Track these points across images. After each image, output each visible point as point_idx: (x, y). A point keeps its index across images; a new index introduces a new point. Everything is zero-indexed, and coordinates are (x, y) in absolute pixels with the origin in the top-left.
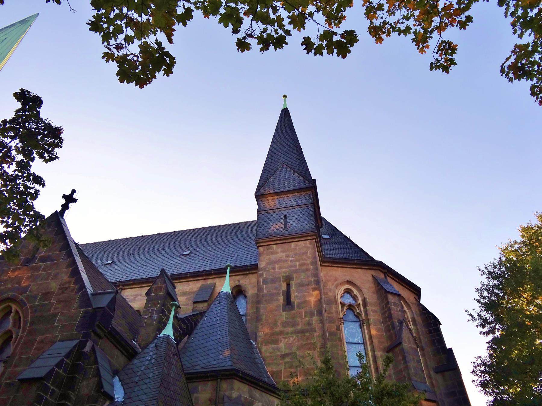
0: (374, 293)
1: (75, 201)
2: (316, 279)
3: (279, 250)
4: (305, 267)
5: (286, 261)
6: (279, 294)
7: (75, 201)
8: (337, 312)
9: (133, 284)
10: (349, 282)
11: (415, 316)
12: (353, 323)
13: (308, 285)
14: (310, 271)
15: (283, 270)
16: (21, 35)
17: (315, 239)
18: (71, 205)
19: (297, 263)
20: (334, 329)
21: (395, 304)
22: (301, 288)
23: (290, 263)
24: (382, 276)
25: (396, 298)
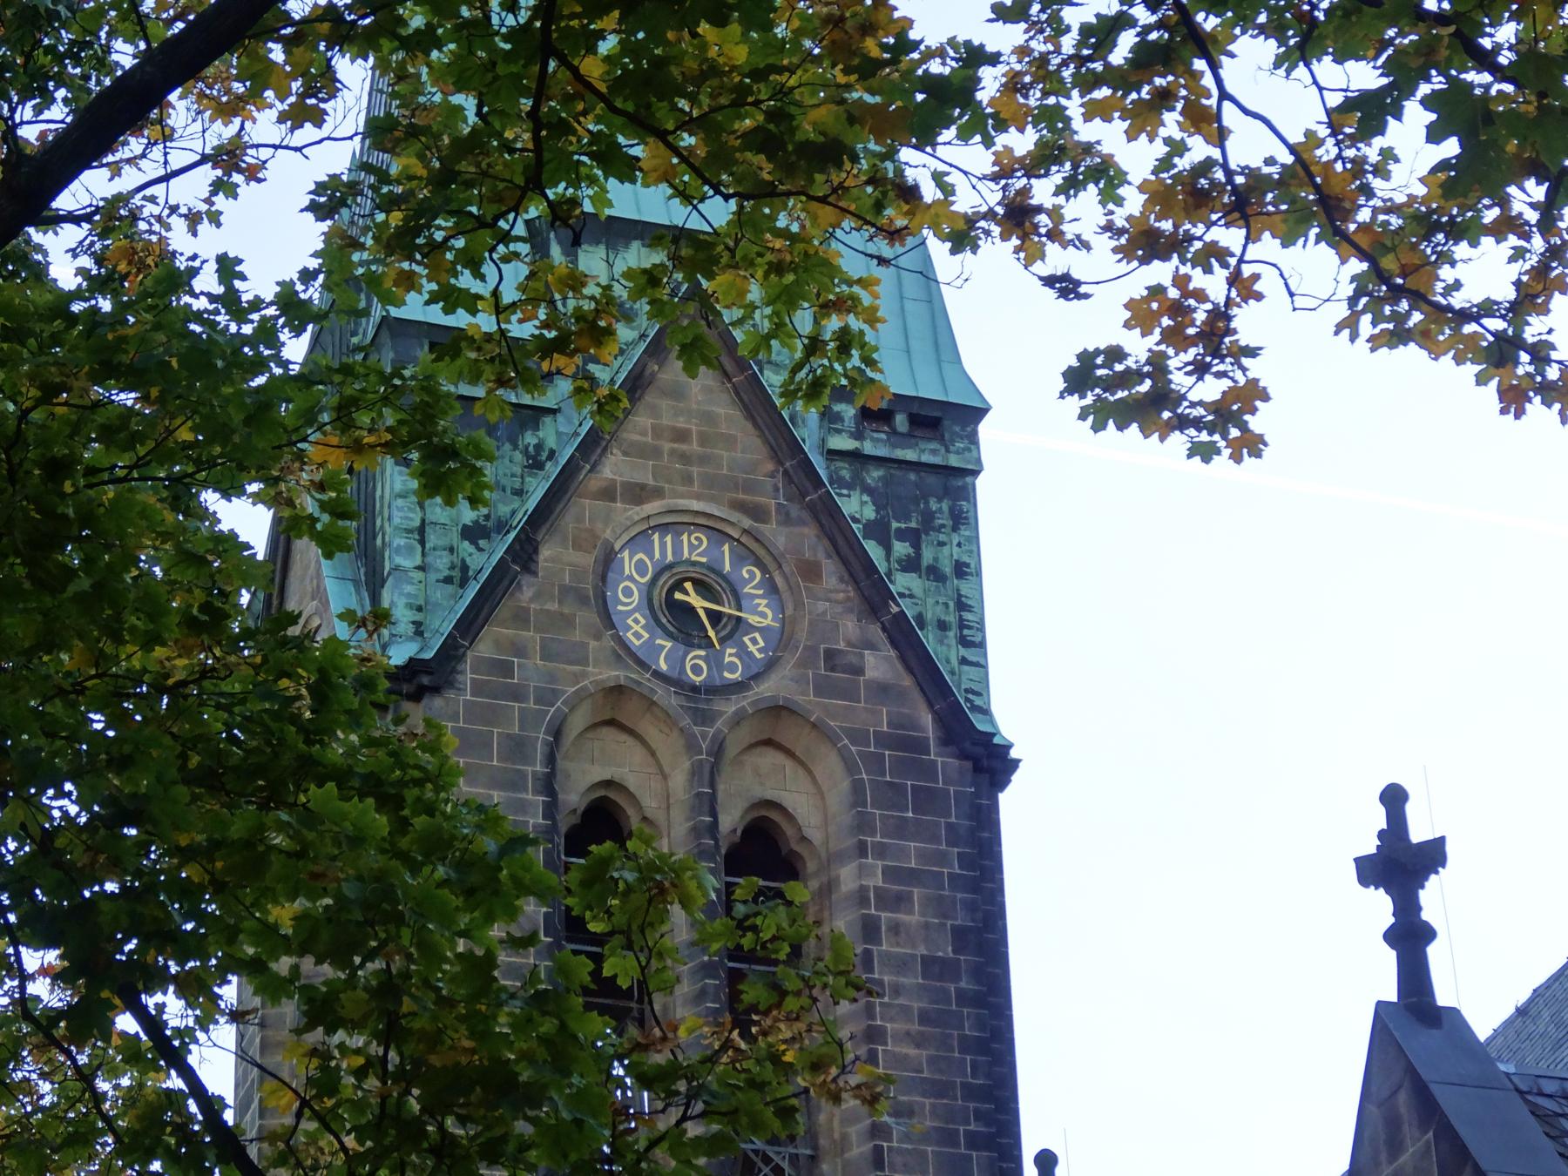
1: (1432, 856)
7: (1432, 856)
18: (1433, 899)
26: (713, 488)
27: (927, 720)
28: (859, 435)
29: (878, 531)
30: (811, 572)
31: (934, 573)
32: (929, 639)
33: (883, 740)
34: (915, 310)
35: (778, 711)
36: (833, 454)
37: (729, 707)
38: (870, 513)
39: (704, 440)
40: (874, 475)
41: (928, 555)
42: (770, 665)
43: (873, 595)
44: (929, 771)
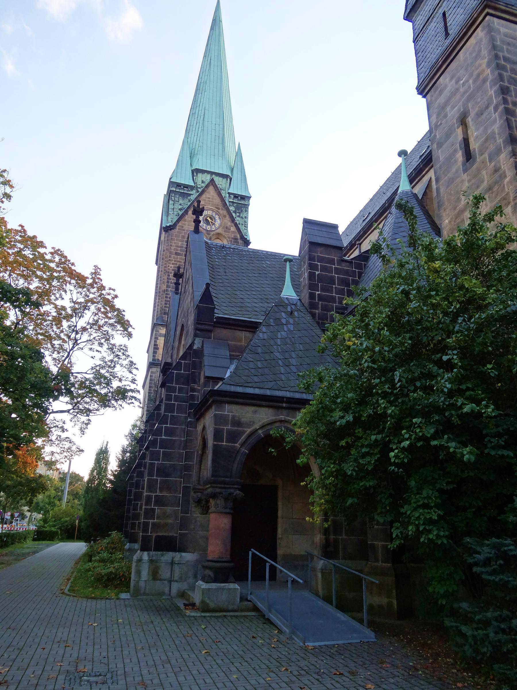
2: (498, 85)
3: (448, 80)
4: (481, 77)
5: (457, 90)
6: (456, 151)
9: (365, 233)
13: (487, 107)
15: (456, 108)
16: (219, 41)
19: (471, 81)
23: (462, 90)
26: (212, 205)
27: (239, 236)
28: (233, 199)
29: (235, 212)
30: (225, 216)
31: (242, 218)
32: (240, 226)
33: (232, 238)
34: (243, 184)
35: (219, 234)
36: (230, 202)
37: (212, 233)
38: (234, 209)
39: (212, 199)
40: (235, 205)
41: (241, 215)
42: (219, 228)
43: (233, 220)
44: (238, 242)
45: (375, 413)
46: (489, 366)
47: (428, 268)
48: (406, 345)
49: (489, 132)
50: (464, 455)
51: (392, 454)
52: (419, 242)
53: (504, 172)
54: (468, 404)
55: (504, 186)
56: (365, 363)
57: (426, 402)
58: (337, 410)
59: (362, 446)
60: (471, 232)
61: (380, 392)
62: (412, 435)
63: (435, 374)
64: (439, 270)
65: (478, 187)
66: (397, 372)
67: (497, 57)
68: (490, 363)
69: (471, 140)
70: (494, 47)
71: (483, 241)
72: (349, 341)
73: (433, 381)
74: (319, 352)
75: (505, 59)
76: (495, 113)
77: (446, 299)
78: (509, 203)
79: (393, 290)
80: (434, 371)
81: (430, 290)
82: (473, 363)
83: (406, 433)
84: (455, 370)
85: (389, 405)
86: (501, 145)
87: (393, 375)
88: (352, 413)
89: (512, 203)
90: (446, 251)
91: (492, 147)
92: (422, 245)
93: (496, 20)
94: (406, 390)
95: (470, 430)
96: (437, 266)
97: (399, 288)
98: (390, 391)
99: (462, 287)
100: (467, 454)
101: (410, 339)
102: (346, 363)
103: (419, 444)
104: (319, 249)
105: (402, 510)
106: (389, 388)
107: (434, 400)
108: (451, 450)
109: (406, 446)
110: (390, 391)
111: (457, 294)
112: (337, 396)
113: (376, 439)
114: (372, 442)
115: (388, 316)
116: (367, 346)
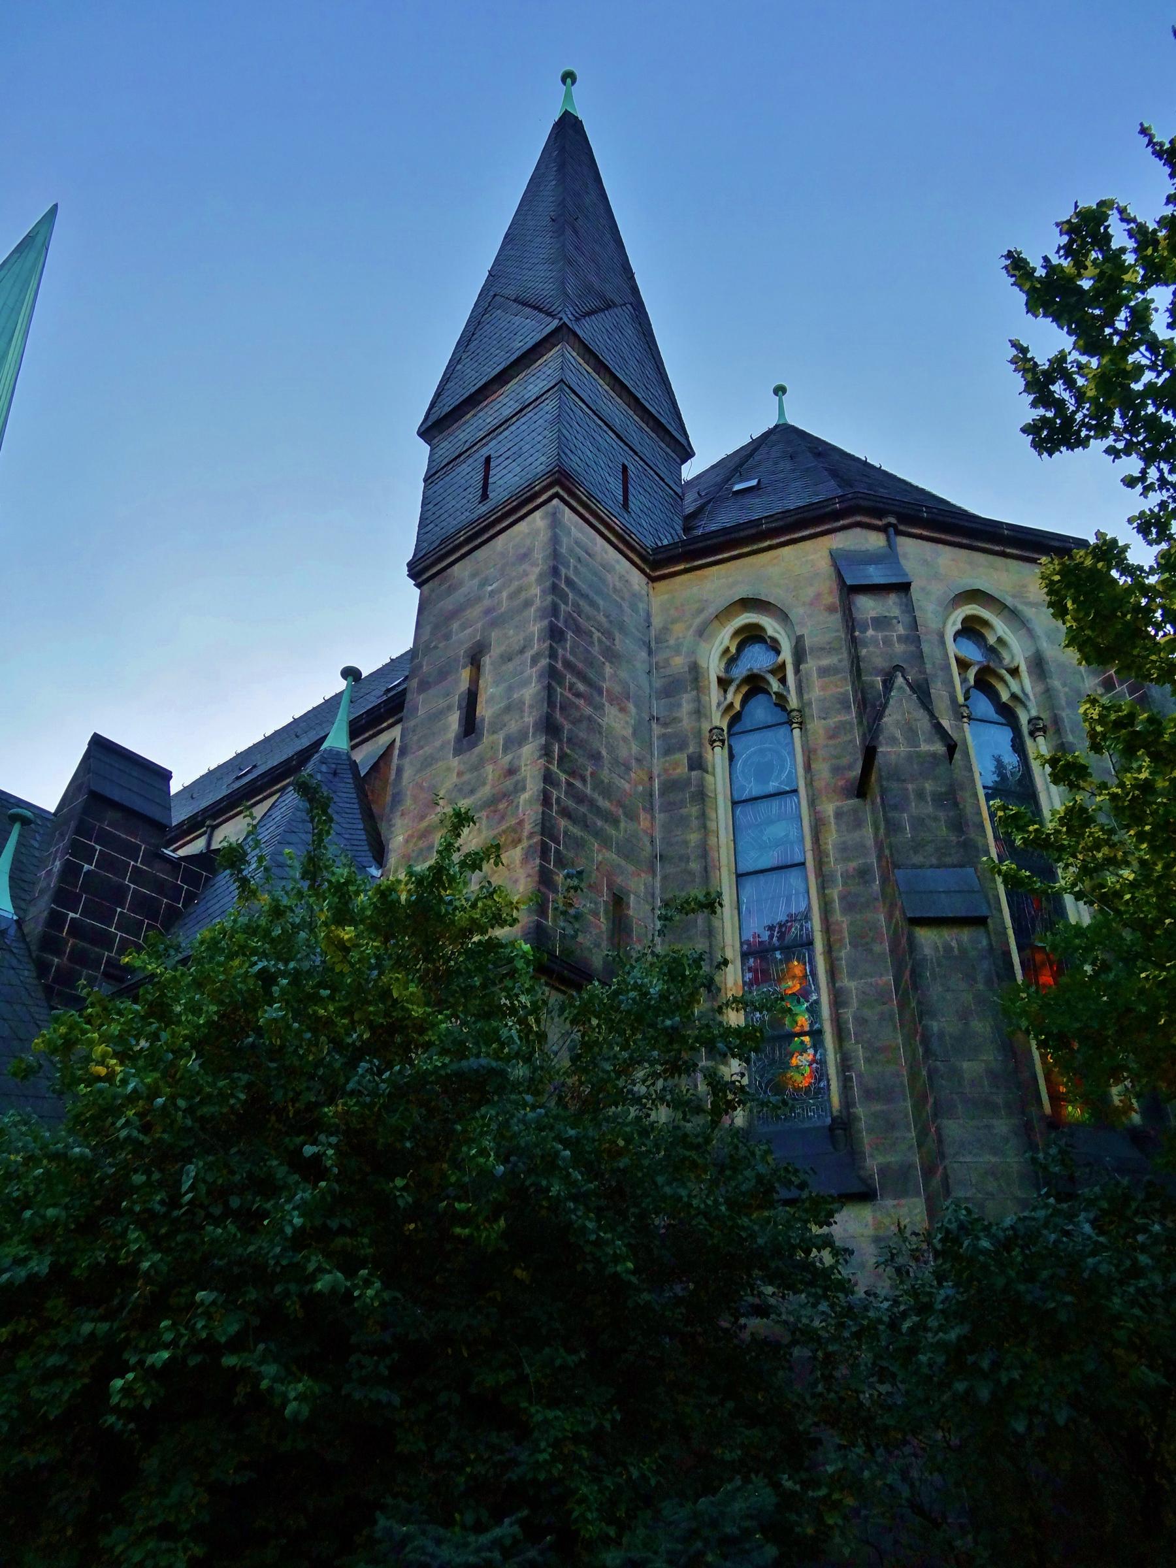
0: (831, 609)
4: (523, 596)
5: (479, 599)
8: (699, 712)
10: (747, 604)
11: (1044, 645)
12: (769, 734)
13: (522, 651)
14: (531, 605)
15: (469, 630)
16: (27, 283)
17: (556, 495)
19: (505, 594)
20: (682, 770)
21: (881, 623)
22: (510, 666)
23: (487, 602)
24: (875, 541)
25: (892, 598)
45: (111, 1262)
46: (400, 1182)
47: (327, 937)
48: (232, 1101)
49: (515, 696)
50: (289, 1401)
51: (118, 1383)
52: (325, 873)
53: (524, 780)
54: (330, 1272)
55: (517, 806)
56: (123, 1127)
57: (240, 1250)
58: (16, 1239)
59: (53, 1348)
60: (431, 884)
61: (137, 1208)
62: (182, 1336)
63: (281, 1183)
64: (348, 944)
65: (472, 792)
66: (192, 1167)
67: (555, 571)
68: (404, 1177)
69: (482, 699)
70: (555, 555)
71: (450, 909)
72: (102, 1063)
73: (269, 1200)
74: (15, 1074)
75: (569, 582)
76: (531, 667)
77: (347, 1012)
78: (520, 841)
79: (241, 966)
80: (279, 1176)
81: (321, 985)
82: (368, 1169)
83: (167, 1329)
84: (323, 1184)
85: (150, 1248)
86: (528, 728)
87: (180, 1172)
88: (51, 1254)
89: (525, 844)
90: (376, 907)
91: (513, 727)
92: (330, 882)
93: (567, 509)
94: (202, 1213)
95: (321, 1336)
96: (346, 937)
97: (255, 963)
98: (163, 1210)
99: (385, 994)
100: (296, 1396)
101: (249, 1086)
102: (77, 1116)
103: (193, 1361)
104: (112, 815)
105: (105, 1541)
106: (162, 1202)
107: (260, 1248)
108: (265, 1384)
109: (159, 1365)
110: (163, 1210)
111: (371, 1009)
112: (26, 1202)
113: (92, 1334)
114: (81, 1341)
115: (210, 1023)
116: (135, 1090)
